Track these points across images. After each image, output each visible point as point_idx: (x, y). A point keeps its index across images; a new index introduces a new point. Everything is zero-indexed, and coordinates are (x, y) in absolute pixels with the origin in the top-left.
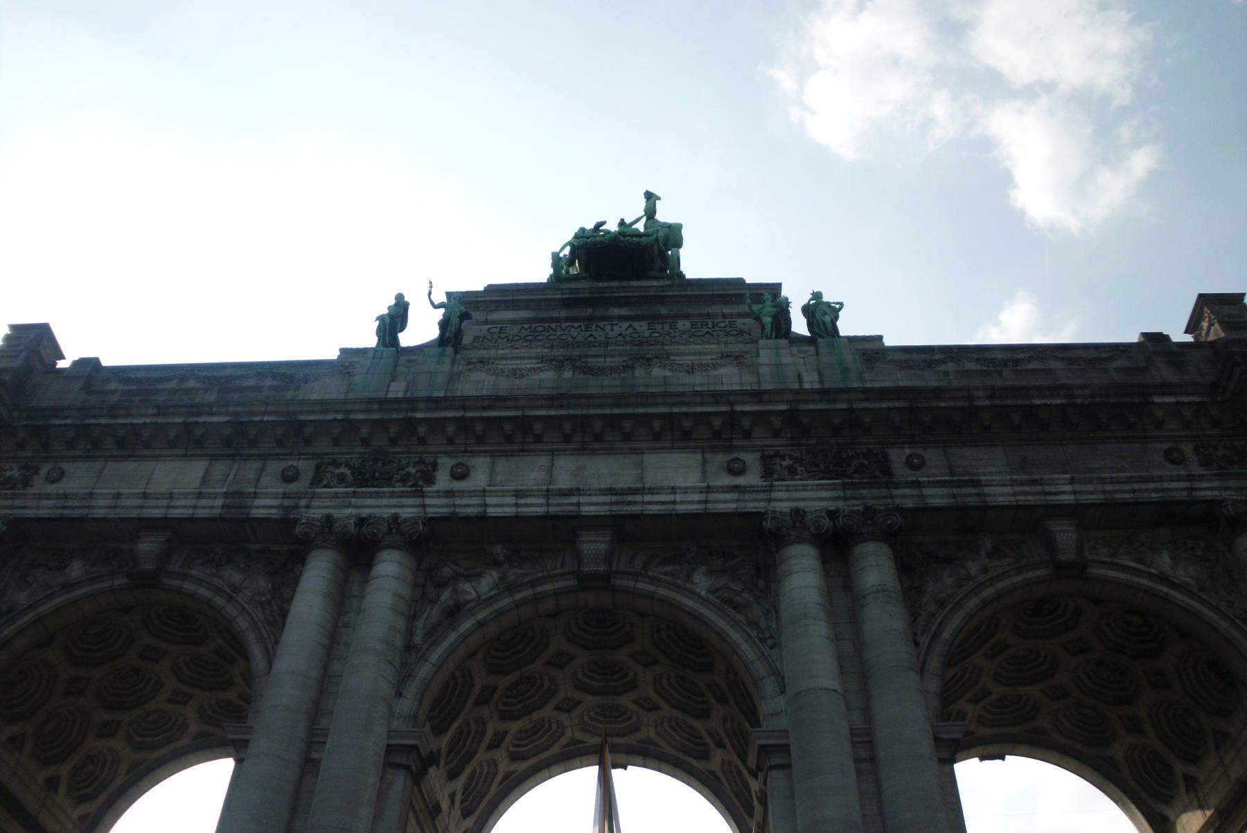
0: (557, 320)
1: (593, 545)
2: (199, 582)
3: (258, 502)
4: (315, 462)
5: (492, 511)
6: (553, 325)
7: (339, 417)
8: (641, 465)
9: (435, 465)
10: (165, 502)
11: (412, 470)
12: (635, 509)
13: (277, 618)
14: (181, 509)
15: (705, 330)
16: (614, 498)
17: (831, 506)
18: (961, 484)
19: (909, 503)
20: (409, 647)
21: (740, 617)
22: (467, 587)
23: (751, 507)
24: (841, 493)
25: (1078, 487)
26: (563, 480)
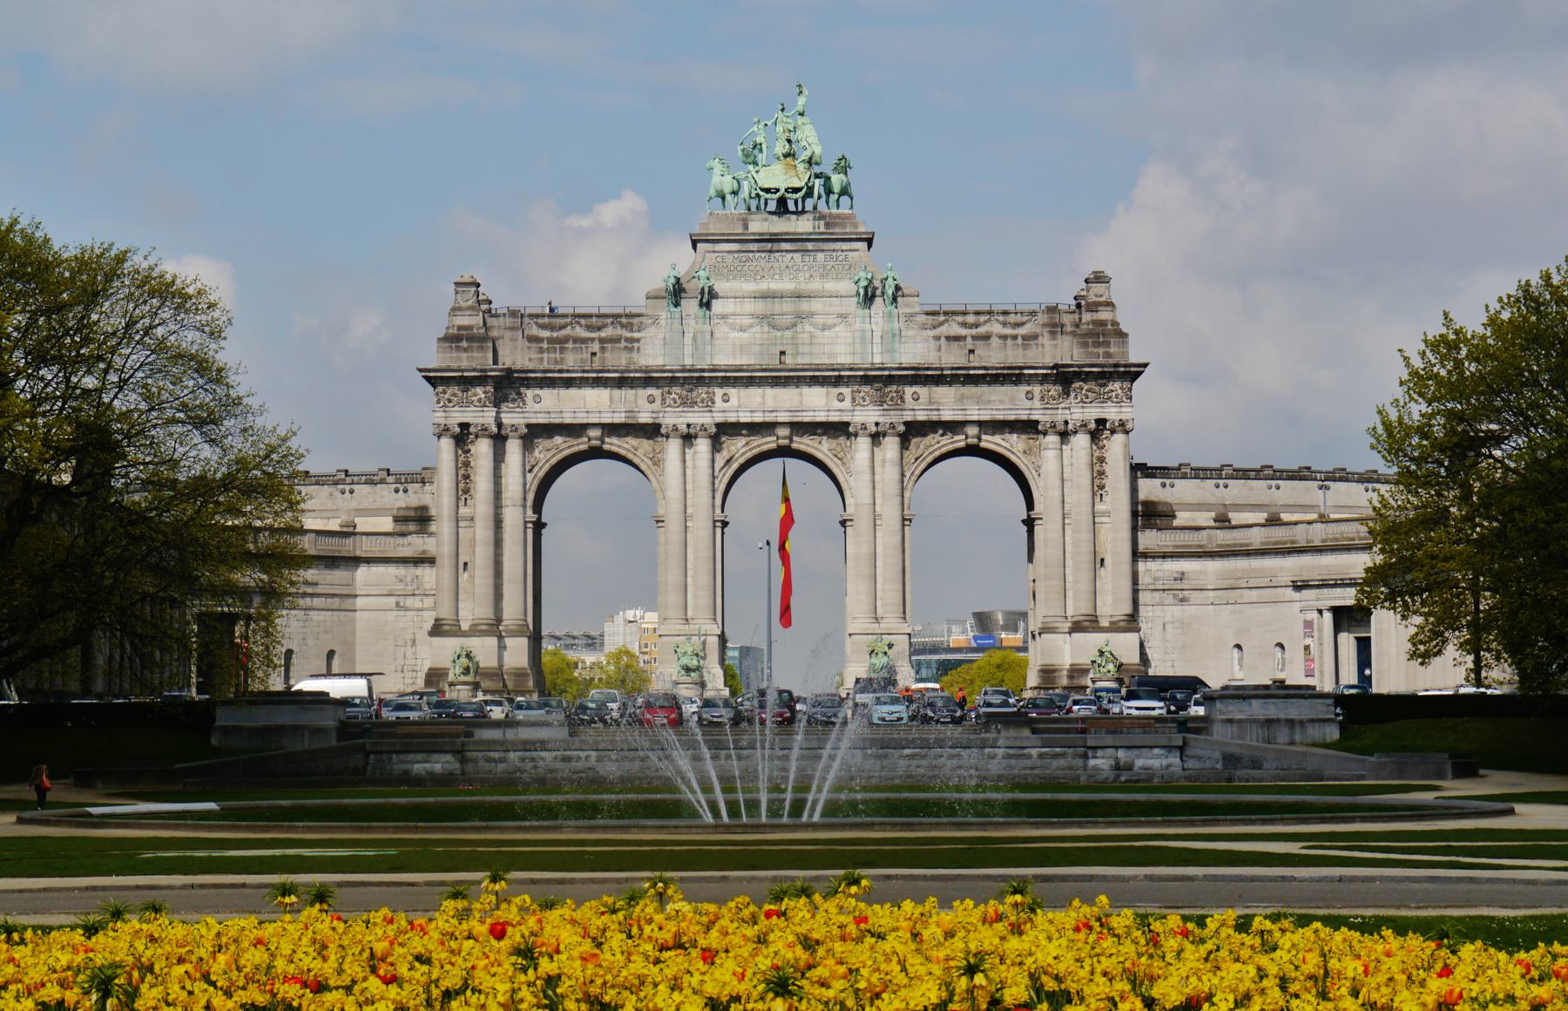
0: (753, 251)
1: (783, 432)
2: (619, 446)
3: (641, 415)
4: (661, 391)
5: (742, 420)
6: (751, 255)
7: (670, 375)
8: (801, 394)
9: (714, 394)
10: (598, 415)
11: (704, 396)
12: (799, 419)
13: (657, 462)
14: (607, 419)
15: (832, 263)
16: (792, 414)
17: (876, 419)
18: (931, 410)
19: (909, 419)
20: (714, 477)
21: (839, 462)
22: (732, 448)
23: (845, 419)
24: (882, 413)
25: (981, 412)
26: (770, 404)
